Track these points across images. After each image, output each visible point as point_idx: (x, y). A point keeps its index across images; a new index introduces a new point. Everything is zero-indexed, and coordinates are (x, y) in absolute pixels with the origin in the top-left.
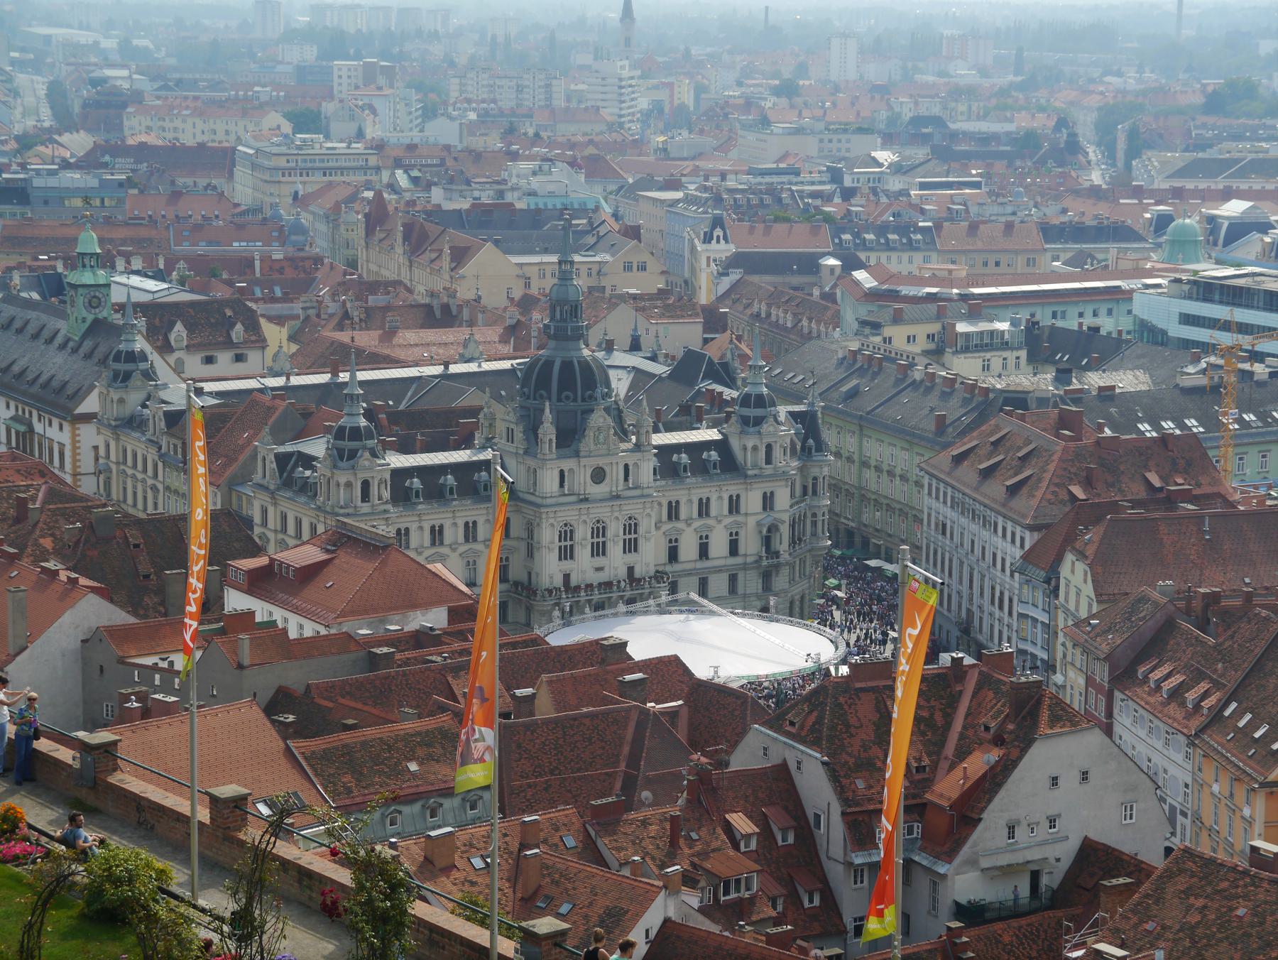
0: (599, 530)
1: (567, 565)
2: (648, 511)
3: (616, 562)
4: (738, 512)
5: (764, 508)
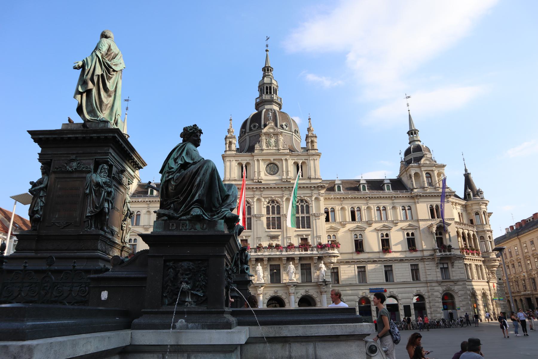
3: (291, 233)
5: (433, 217)
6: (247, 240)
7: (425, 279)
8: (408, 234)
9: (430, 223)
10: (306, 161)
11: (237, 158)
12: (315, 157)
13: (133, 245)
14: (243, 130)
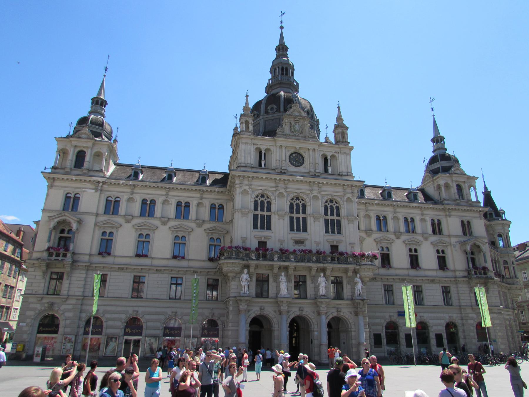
0: (298, 206)
1: (263, 234)
2: (349, 196)
4: (440, 233)
5: (465, 234)
6: (266, 242)
7: (457, 304)
8: (438, 251)
9: (462, 239)
10: (335, 154)
11: (255, 142)
12: (347, 151)
13: (107, 240)
14: (256, 112)
